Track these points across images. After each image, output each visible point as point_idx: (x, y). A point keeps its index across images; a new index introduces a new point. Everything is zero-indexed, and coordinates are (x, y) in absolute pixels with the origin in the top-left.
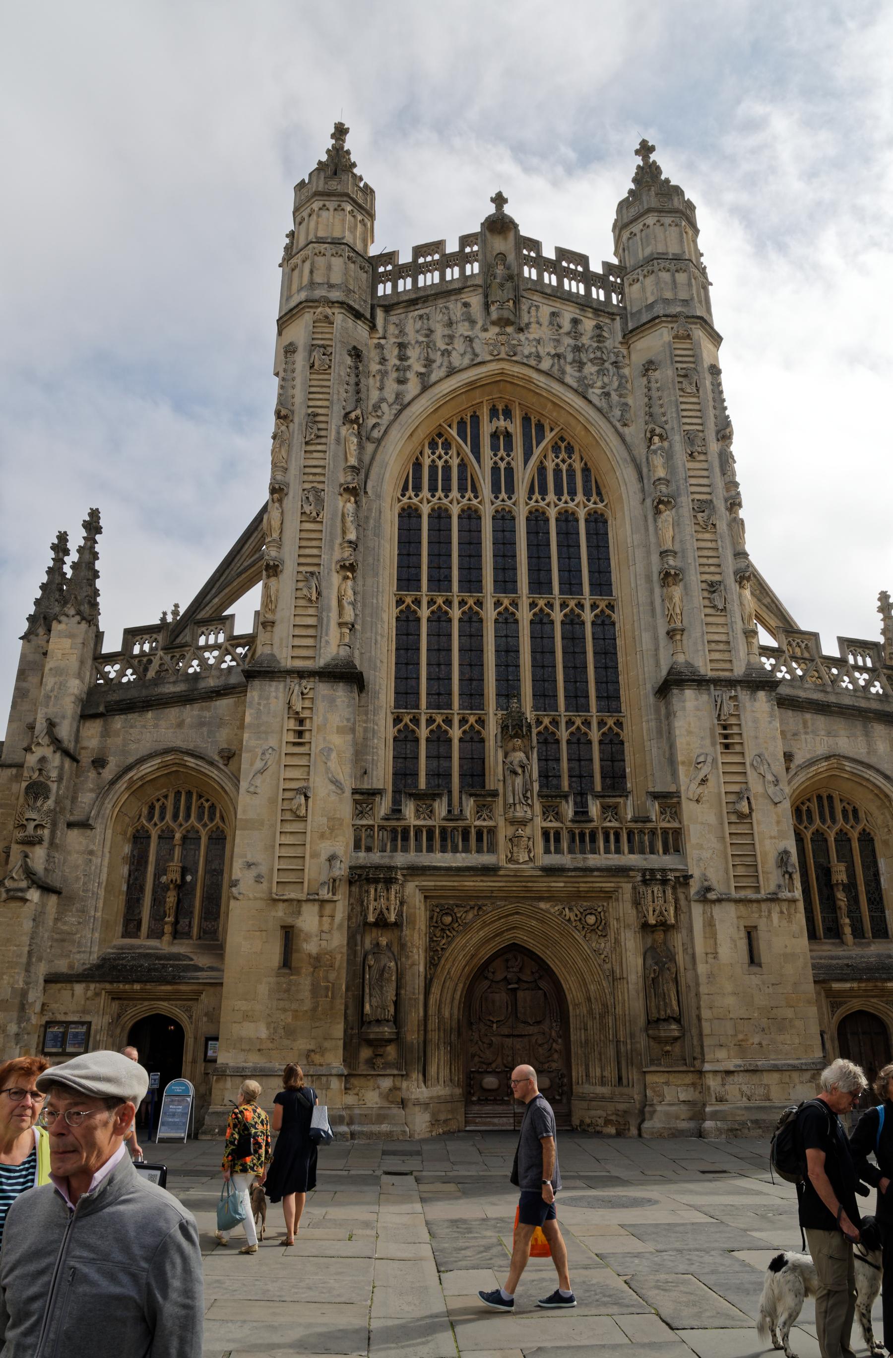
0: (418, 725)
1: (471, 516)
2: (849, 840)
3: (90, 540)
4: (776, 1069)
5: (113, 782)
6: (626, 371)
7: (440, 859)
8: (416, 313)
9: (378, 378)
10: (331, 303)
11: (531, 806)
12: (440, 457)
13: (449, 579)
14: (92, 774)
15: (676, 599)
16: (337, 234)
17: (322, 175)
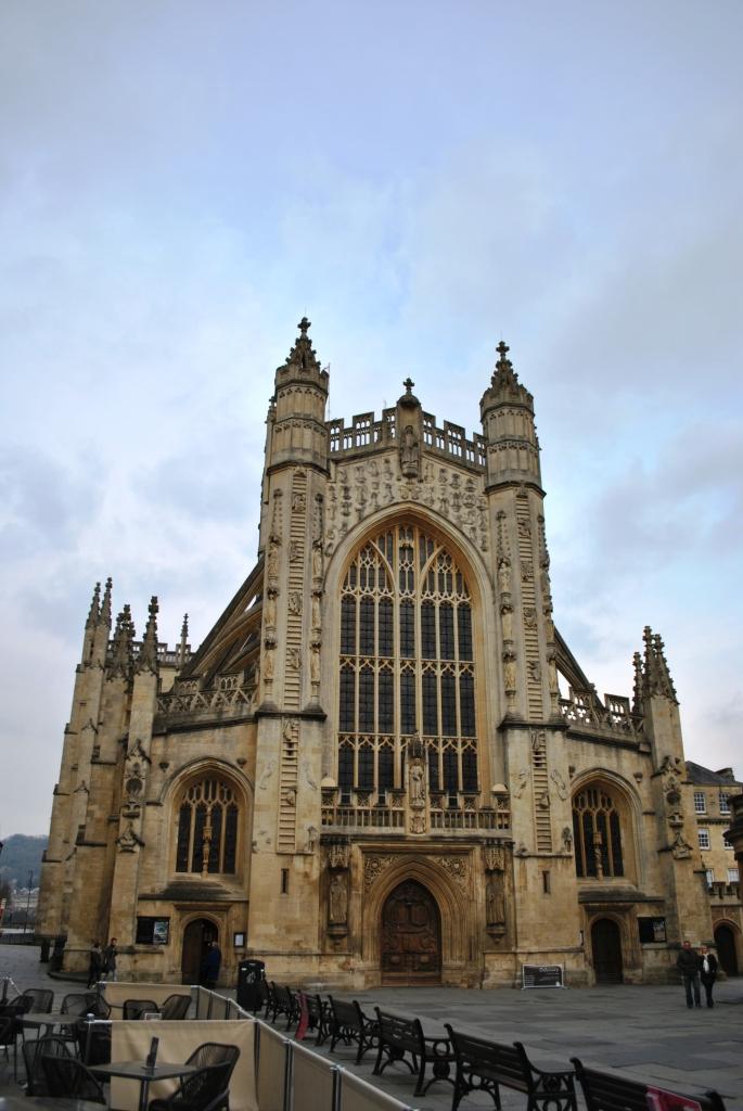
1: (387, 602)
2: (604, 817)
3: (153, 618)
4: (555, 952)
5: (173, 777)
6: (487, 512)
8: (355, 466)
9: (331, 511)
10: (306, 464)
12: (368, 563)
13: (373, 646)
14: (160, 772)
15: (512, 672)
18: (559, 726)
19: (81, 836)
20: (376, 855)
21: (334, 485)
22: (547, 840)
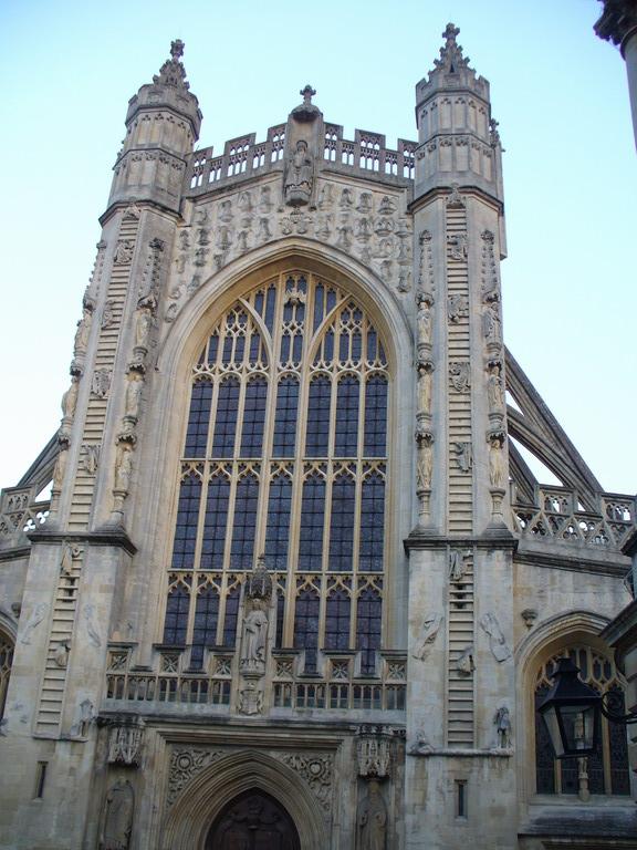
0: (190, 584)
1: (258, 382)
6: (409, 241)
7: (180, 708)
9: (180, 262)
11: (264, 662)
15: (426, 462)
16: (154, 141)
17: (147, 91)
18: (501, 542)
20: (191, 749)
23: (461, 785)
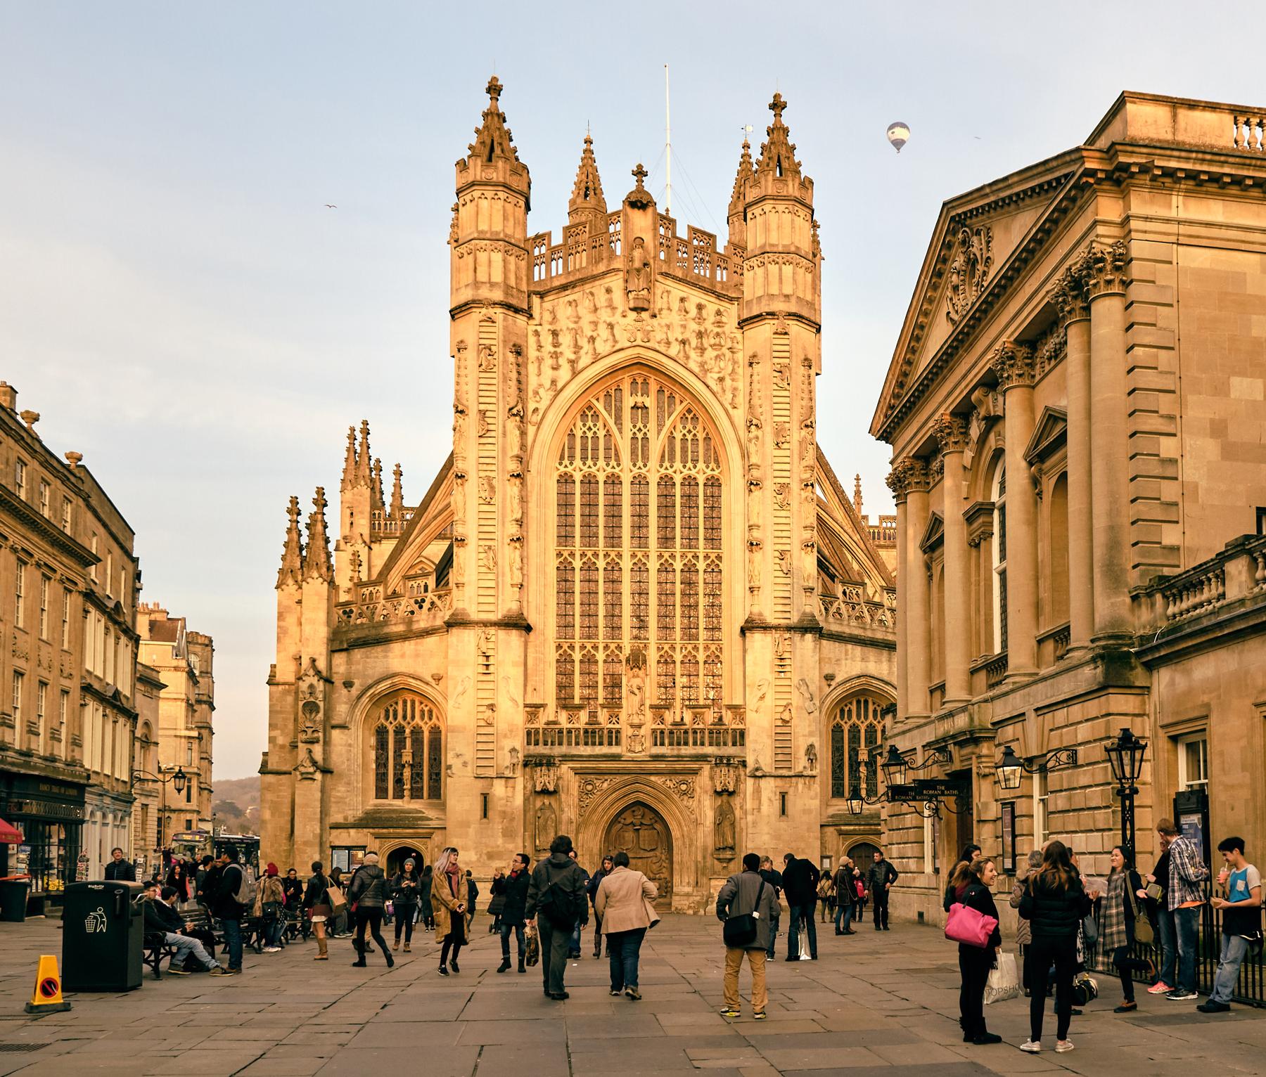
5: (359, 698)
8: (567, 299)
9: (536, 365)
14: (344, 691)
15: (756, 564)
19: (264, 764)
21: (539, 328)
22: (788, 758)
23: (783, 796)
